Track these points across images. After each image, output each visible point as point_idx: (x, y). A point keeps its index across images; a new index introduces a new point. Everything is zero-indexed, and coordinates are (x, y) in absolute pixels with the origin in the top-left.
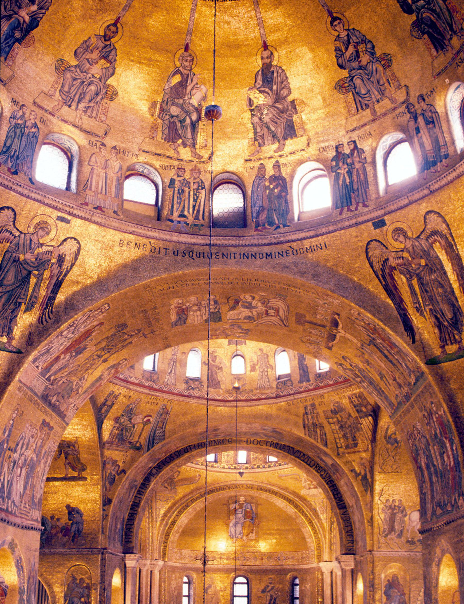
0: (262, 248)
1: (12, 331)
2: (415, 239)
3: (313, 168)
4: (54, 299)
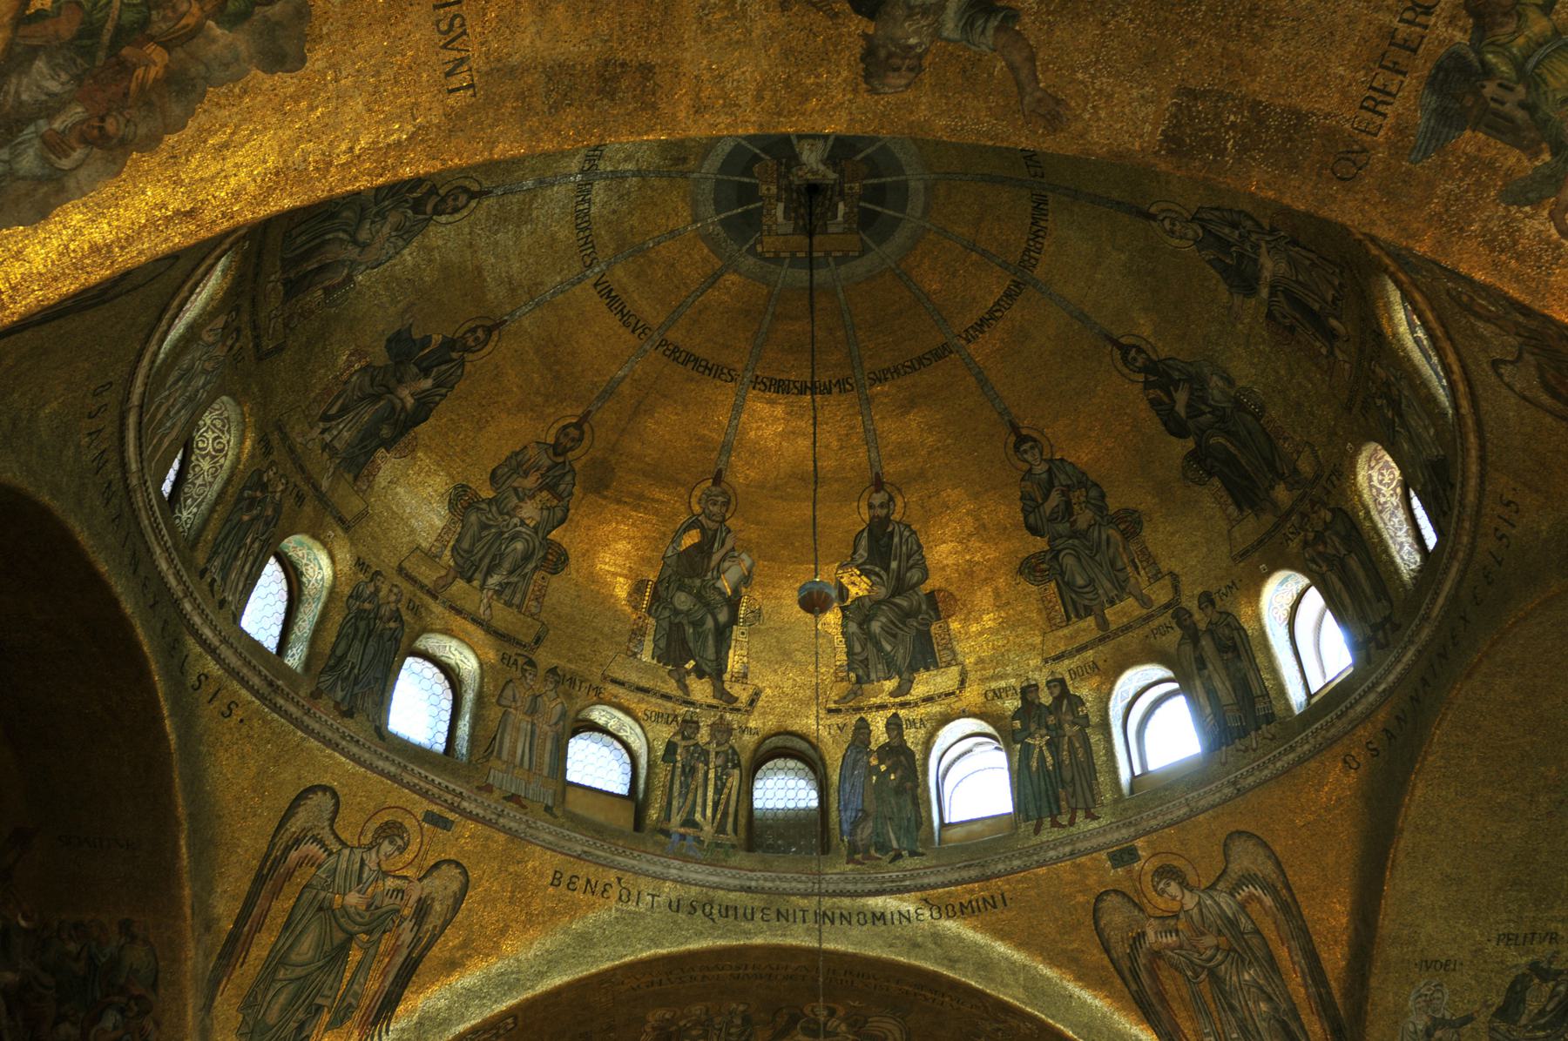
3: (968, 732)
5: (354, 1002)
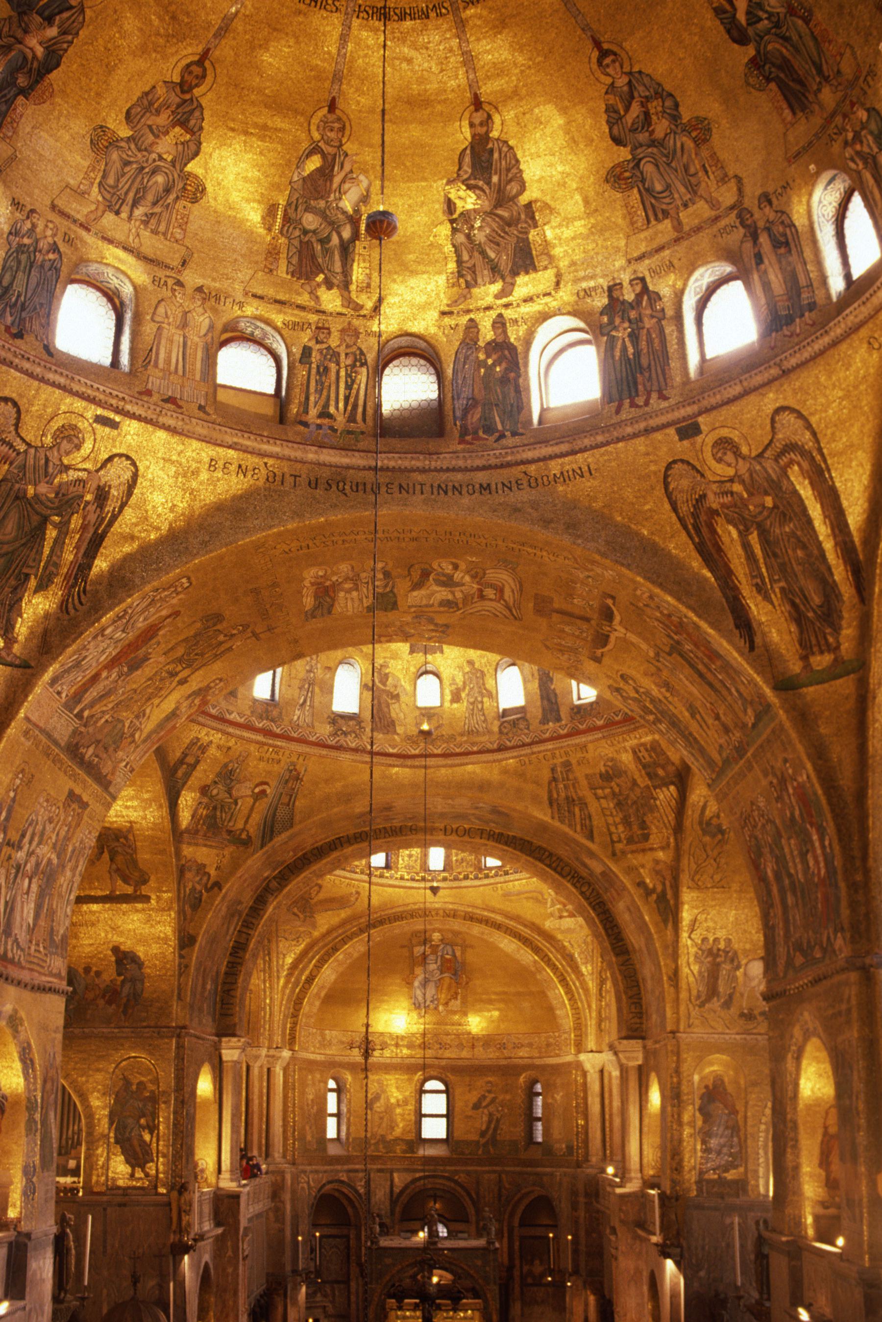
0: (472, 474)
1: (13, 627)
2: (754, 458)
3: (566, 328)
4: (90, 567)
5: (53, 569)
